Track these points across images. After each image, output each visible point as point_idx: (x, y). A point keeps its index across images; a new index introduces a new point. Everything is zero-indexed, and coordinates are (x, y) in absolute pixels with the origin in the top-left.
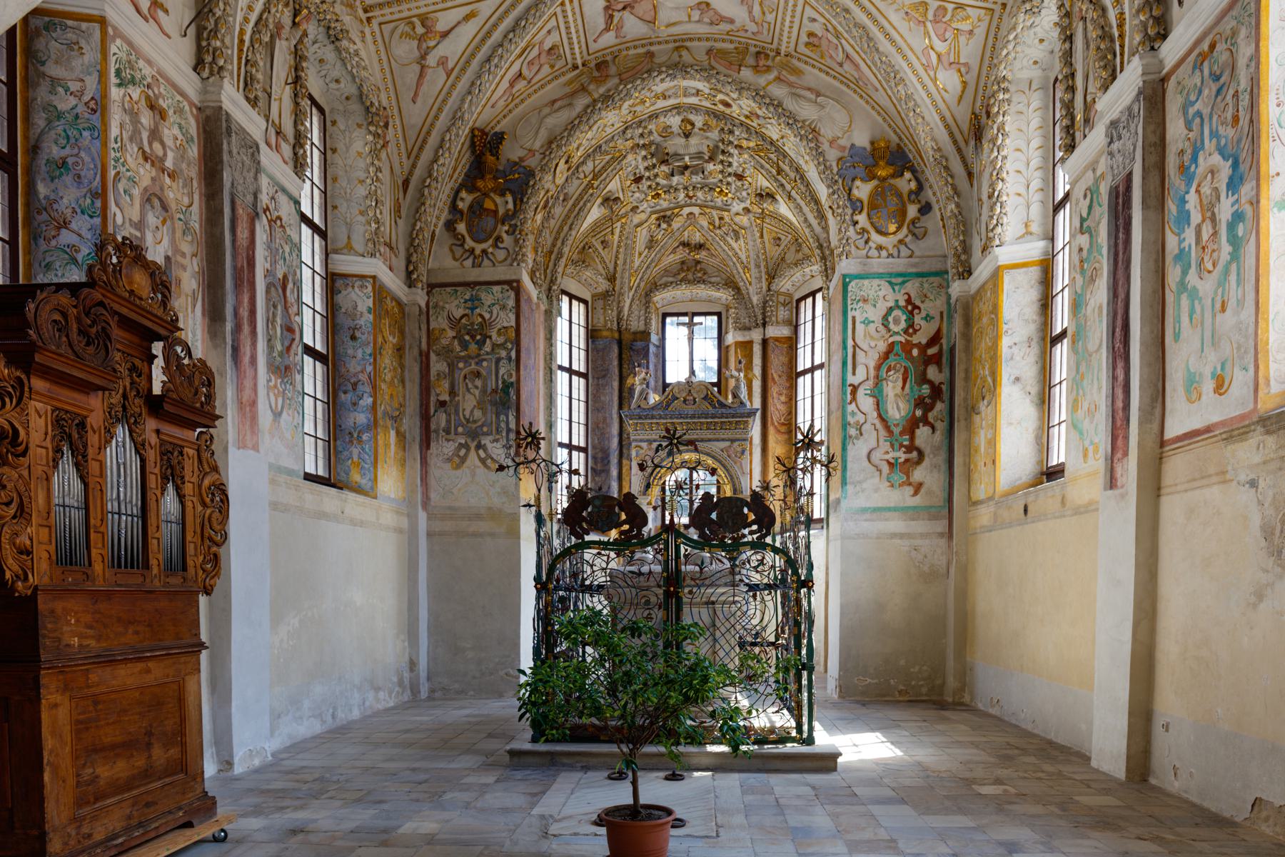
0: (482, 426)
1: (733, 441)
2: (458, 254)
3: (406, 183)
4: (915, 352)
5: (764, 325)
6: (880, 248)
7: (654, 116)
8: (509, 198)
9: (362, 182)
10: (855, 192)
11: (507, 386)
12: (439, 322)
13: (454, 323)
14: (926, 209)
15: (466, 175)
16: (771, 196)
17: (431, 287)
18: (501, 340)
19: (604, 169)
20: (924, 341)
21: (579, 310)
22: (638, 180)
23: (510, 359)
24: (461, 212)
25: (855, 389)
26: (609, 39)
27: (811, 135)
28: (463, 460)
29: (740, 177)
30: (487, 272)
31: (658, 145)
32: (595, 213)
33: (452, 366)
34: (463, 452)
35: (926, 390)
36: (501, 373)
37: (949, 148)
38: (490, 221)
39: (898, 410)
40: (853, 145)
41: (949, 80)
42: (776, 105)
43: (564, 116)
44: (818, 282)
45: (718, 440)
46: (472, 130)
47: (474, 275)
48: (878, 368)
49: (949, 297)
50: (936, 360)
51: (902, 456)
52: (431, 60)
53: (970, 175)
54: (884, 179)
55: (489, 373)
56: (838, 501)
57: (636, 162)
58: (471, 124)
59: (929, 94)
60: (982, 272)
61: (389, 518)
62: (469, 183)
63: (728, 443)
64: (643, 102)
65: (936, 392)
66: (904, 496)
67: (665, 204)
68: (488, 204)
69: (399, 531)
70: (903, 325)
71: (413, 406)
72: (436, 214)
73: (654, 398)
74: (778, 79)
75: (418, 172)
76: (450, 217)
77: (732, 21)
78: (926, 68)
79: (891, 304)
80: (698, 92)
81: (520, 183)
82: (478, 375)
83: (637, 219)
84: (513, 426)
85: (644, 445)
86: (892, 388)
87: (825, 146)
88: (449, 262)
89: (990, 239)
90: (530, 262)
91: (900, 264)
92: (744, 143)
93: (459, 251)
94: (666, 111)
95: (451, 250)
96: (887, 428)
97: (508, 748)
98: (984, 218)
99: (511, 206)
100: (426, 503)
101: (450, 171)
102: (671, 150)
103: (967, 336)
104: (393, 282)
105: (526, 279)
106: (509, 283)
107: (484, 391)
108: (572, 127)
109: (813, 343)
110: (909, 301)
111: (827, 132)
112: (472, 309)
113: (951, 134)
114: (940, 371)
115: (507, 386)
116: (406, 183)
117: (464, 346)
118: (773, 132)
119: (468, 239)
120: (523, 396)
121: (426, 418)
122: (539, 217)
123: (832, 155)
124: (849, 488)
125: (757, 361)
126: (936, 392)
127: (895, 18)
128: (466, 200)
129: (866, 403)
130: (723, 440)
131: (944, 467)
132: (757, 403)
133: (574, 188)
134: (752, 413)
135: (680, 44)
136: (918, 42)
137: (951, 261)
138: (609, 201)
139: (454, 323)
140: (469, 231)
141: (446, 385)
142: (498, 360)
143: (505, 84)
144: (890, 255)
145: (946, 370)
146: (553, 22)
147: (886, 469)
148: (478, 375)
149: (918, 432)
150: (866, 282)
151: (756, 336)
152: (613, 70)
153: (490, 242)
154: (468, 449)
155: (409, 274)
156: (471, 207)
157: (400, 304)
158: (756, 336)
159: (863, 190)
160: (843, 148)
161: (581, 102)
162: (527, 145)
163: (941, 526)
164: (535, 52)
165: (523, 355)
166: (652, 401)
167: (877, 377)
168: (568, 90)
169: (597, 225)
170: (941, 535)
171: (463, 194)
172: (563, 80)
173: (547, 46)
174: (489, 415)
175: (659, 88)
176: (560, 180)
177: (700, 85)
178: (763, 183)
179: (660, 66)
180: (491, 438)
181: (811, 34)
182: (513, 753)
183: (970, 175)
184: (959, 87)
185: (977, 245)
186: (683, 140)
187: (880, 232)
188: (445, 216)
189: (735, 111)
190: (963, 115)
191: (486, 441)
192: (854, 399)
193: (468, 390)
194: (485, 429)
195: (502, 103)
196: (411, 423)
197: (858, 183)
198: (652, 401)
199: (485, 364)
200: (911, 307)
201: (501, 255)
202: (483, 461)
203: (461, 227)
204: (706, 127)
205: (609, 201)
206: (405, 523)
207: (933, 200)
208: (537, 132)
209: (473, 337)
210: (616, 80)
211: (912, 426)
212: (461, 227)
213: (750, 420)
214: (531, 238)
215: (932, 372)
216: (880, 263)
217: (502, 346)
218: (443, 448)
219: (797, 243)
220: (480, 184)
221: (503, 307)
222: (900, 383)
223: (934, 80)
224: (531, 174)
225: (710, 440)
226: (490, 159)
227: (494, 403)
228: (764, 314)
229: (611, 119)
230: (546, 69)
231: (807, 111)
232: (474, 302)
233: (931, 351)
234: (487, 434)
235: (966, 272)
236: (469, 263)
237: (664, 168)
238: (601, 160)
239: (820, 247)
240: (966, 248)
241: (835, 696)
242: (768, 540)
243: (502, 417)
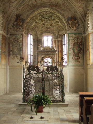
1: (53, 55)
3: (7, 21)
4: (78, 44)
5: (58, 38)
6: (73, 30)
7: (42, 12)
9: (1, 21)
10: (69, 23)
12: (11, 39)
13: (14, 39)
14: (79, 25)
16: (58, 22)
17: (10, 35)
18: (20, 42)
19: (35, 18)
20: (79, 42)
21: (32, 36)
22: (40, 20)
25: (70, 48)
26: (35, 3)
27: (63, 15)
28: (14, 58)
29: (54, 19)
30: (18, 33)
31: (43, 16)
32: (34, 24)
33: (13, 45)
34: (14, 57)
35: (80, 49)
37: (82, 17)
38: (19, 26)
39: (76, 52)
40: (69, 17)
41: (81, 9)
42: (58, 11)
43: (30, 12)
44: (65, 33)
46: (17, 14)
47: (16, 33)
48: (73, 46)
49: (82, 36)
50: (81, 45)
51: (77, 58)
52: (11, 6)
53: (84, 21)
54: (73, 21)
55: (18, 46)
56: (68, 64)
57: (40, 18)
59: (78, 11)
60: (87, 33)
61: (3, 67)
64: (40, 11)
65: (81, 49)
66: (78, 63)
67: (44, 23)
68: (19, 24)
69: (4, 68)
70: (76, 40)
71: (7, 51)
72: (11, 25)
73: (42, 49)
74: (58, 8)
75: (9, 20)
77: (52, 1)
78: (78, 7)
79: (75, 37)
80: (48, 10)
81: (23, 21)
82: (17, 46)
83: (40, 25)
84: (21, 53)
85: (41, 55)
86: (75, 49)
87: (65, 17)
88: (13, 31)
89: (88, 29)
90: (24, 31)
91: (76, 32)
92: (54, 15)
94: (43, 12)
96: (75, 54)
97: (19, 104)
98: (87, 26)
100: (9, 64)
102: (44, 16)
103: (85, 42)
104: (5, 34)
105: (24, 33)
106: (21, 34)
107: (17, 48)
108: (30, 14)
109: (65, 41)
110: (77, 37)
111: (65, 15)
112: (16, 38)
113: (82, 16)
114: (82, 46)
115: (21, 48)
116: (7, 21)
117: (15, 42)
118: (58, 15)
120: (23, 49)
121: (9, 52)
122: (26, 25)
123: (66, 18)
124: (70, 62)
125: (57, 43)
126: (81, 49)
127: (73, 1)
128: (16, 23)
129: (72, 50)
131: (83, 59)
132: (57, 50)
133: (31, 21)
134: (56, 51)
135: (45, 4)
136: (77, 4)
137: (82, 32)
138: (36, 22)
139: (14, 39)
140: (16, 27)
141: (12, 48)
142: (20, 45)
143: (21, 9)
144: (74, 31)
145: (82, 46)
146: (28, 1)
147: (75, 60)
148: (17, 46)
149: (79, 54)
150: (71, 34)
151: (57, 40)
152: (36, 7)
154: (15, 56)
155: (7, 33)
157: (6, 37)
158: (57, 40)
159: (70, 22)
160: (67, 17)
161: (31, 11)
163: (83, 67)
164: (25, 5)
166: (42, 49)
167: (73, 47)
168: (30, 9)
169: (34, 26)
170: (83, 69)
171: (15, 22)
172: (29, 8)
173: (27, 4)
175: (42, 9)
176: (29, 20)
177: (48, 9)
178: (57, 20)
179: (42, 6)
181: (63, 3)
182: (20, 105)
183: (84, 21)
184: (82, 10)
185: (86, 30)
186: (46, 15)
187: (72, 28)
189: (53, 12)
190: (83, 13)
191: (18, 56)
192: (70, 50)
193: (15, 49)
195: (21, 11)
196: (7, 53)
197: (69, 21)
198: (42, 49)
200: (77, 38)
201: (20, 30)
202: (17, 58)
203: (15, 27)
204: (49, 13)
205: (36, 22)
206: (6, 67)
207: (80, 24)
209: (16, 41)
210: (36, 8)
211: (78, 54)
212: (15, 27)
215: (81, 46)
216: (73, 32)
218: (11, 56)
219: (62, 28)
221: (20, 37)
222: (76, 48)
223: (79, 9)
224: (25, 20)
226: (19, 18)
228: (58, 37)
229: (36, 13)
230: (27, 7)
231: (62, 12)
232: (16, 37)
233: (80, 44)
235: (85, 33)
236: (16, 31)
237: (43, 18)
238: (34, 18)
239: (65, 29)
240: (85, 30)
241: (69, 92)
242: (57, 72)
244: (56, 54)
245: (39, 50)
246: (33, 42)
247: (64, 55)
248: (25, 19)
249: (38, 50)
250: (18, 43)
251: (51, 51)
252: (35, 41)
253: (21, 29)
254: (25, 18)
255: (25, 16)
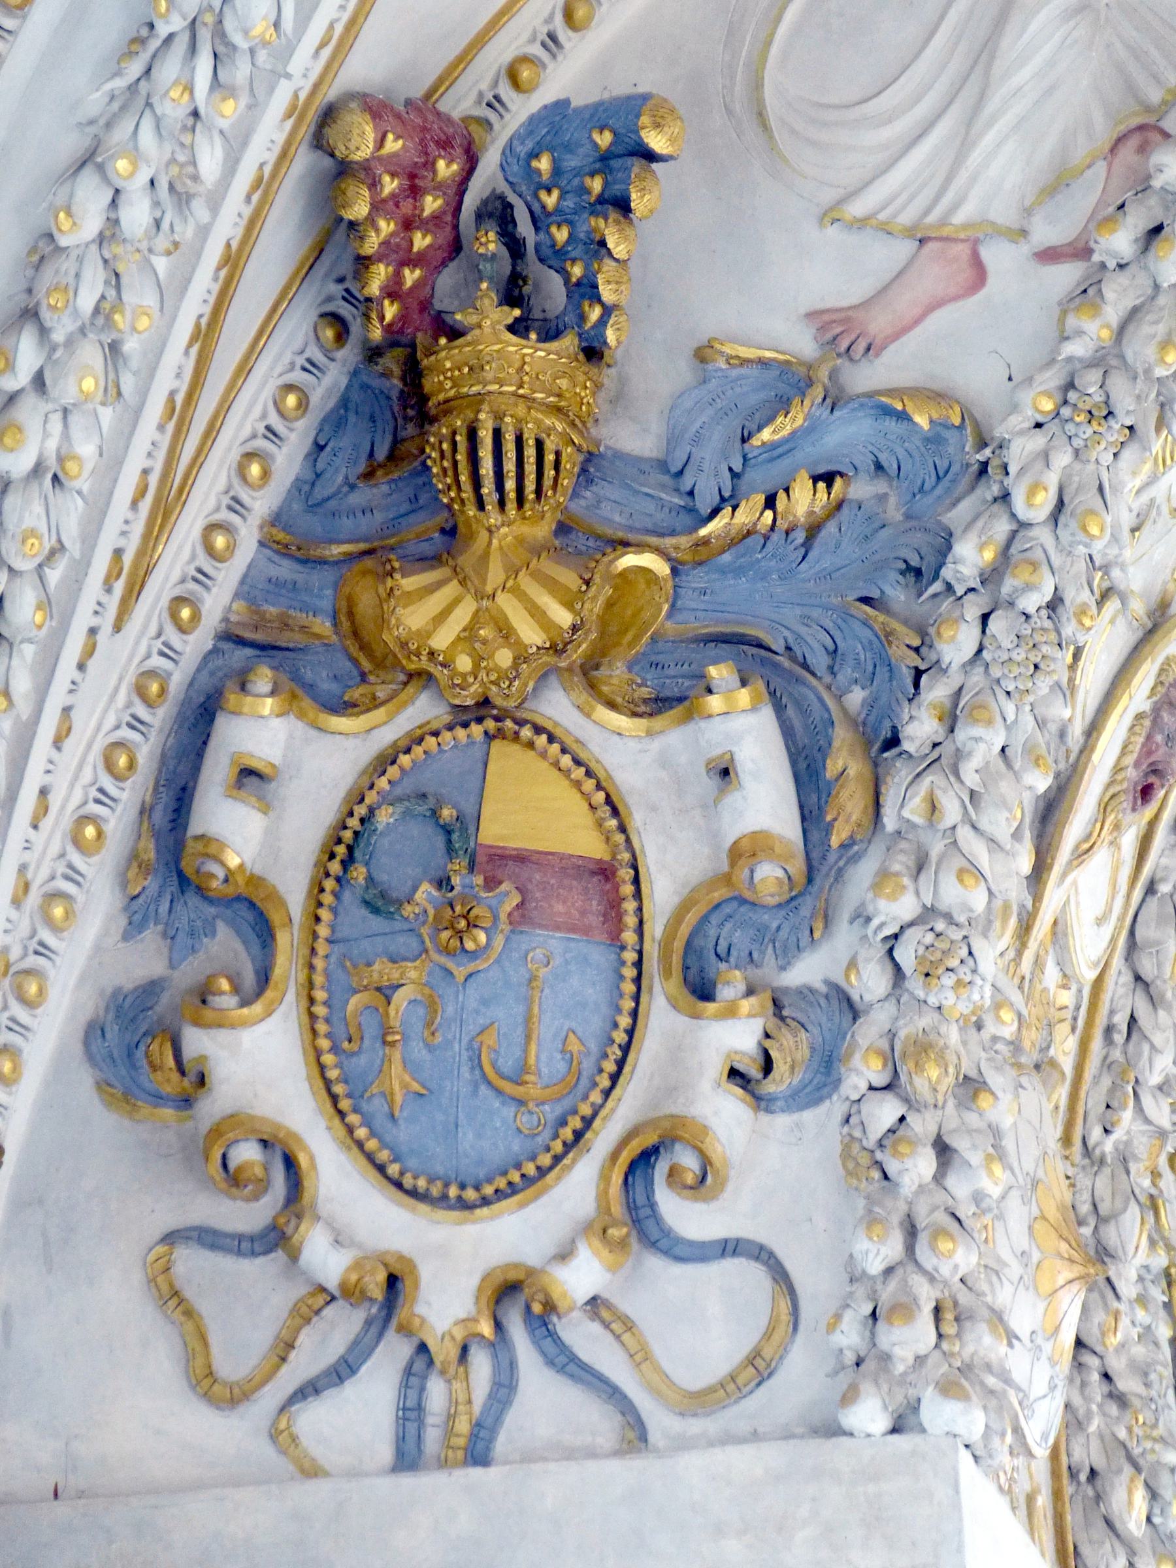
2: (237, 1350)
8: (742, 725)
15: (286, 541)
24: (253, 910)
58: (304, 66)
62: (308, 628)
68: (528, 807)
76: (145, 960)
90: (1041, 1390)
93: (244, 1303)
95: (173, 1299)
99: (766, 802)
101: (123, 525)
119: (335, 1173)
128: (294, 778)
153: (580, 1186)
156: (346, 846)
162: (898, 189)
171: (259, 728)
188: (90, 954)
201: (698, 1319)
203: (260, 1061)
208: (984, 55)
212: (260, 1061)
214: (1024, 1114)
220: (427, 612)
226: (500, 366)
236: (361, 1413)
248: (978, 377)
253: (770, 1170)
254: (973, 347)
255: (997, 175)
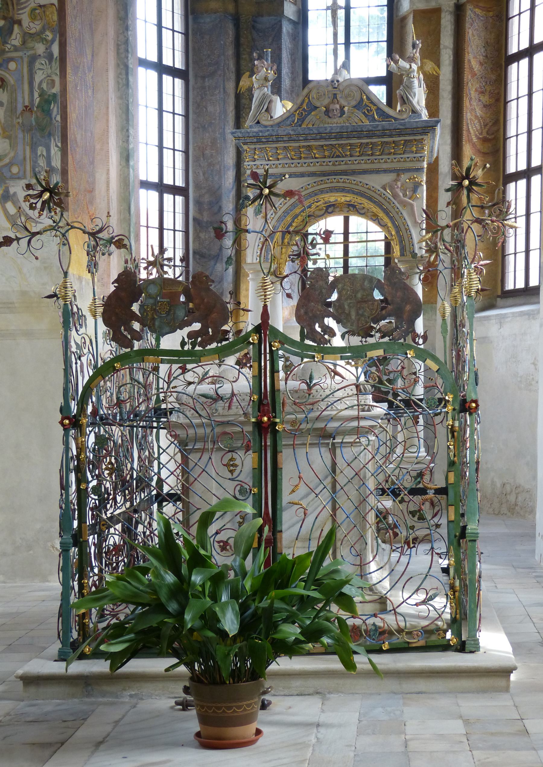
0: (11, 164)
1: (398, 172)
11: (47, 100)
18: (36, 27)
23: (50, 57)
36: (39, 77)
45: (377, 172)
63: (392, 176)
84: (57, 163)
115: (47, 100)
130: (385, 171)
134: (428, 129)
142: (33, 59)
165: (71, 50)
174: (20, 148)
180: (23, 183)
194: (15, 170)
199: (12, 66)
213: (427, 139)
217: (38, 36)
225: (365, 172)
227: (27, 129)
234: (18, 178)
243: (41, 150)
244: (433, 168)
245: (249, 122)
246: (186, 34)
247: (517, 176)
249: (238, 124)
250: (16, 39)
251: (371, 134)
252: (207, 21)
